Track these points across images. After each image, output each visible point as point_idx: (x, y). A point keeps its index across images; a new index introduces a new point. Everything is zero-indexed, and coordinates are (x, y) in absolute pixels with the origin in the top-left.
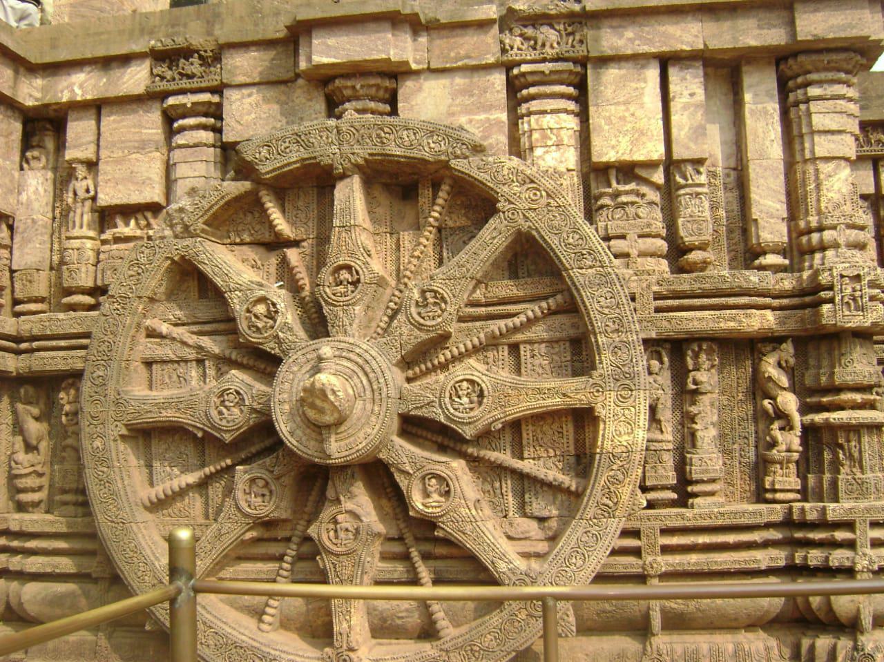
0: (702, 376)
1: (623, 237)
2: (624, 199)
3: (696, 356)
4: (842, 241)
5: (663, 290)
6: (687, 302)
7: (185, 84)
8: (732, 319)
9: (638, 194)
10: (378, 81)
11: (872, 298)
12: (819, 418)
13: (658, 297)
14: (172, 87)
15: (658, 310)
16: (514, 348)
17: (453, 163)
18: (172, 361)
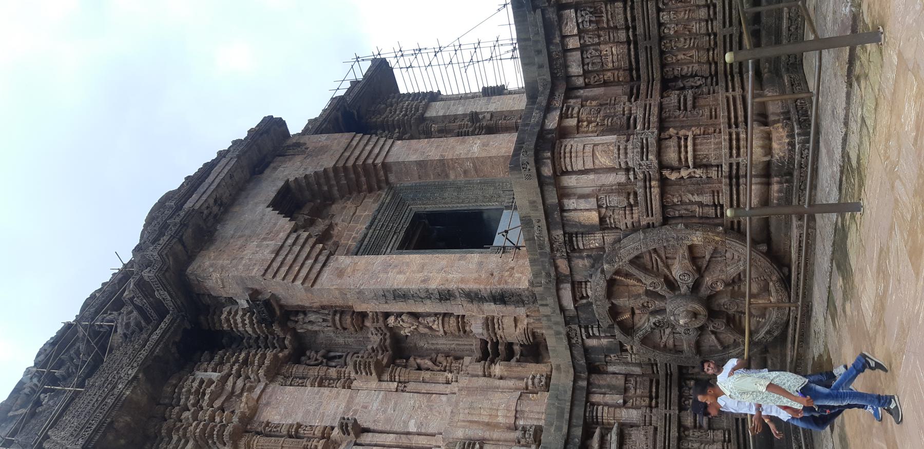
0: (675, 200)
1: (626, 223)
2: (612, 221)
3: (667, 202)
4: (625, 160)
5: (645, 214)
6: (649, 209)
7: (579, 334)
8: (655, 196)
9: (610, 218)
10: (576, 289)
11: (647, 159)
12: (690, 164)
13: (648, 216)
14: (580, 338)
15: (652, 216)
16: (667, 258)
17: (608, 279)
18: (674, 340)
